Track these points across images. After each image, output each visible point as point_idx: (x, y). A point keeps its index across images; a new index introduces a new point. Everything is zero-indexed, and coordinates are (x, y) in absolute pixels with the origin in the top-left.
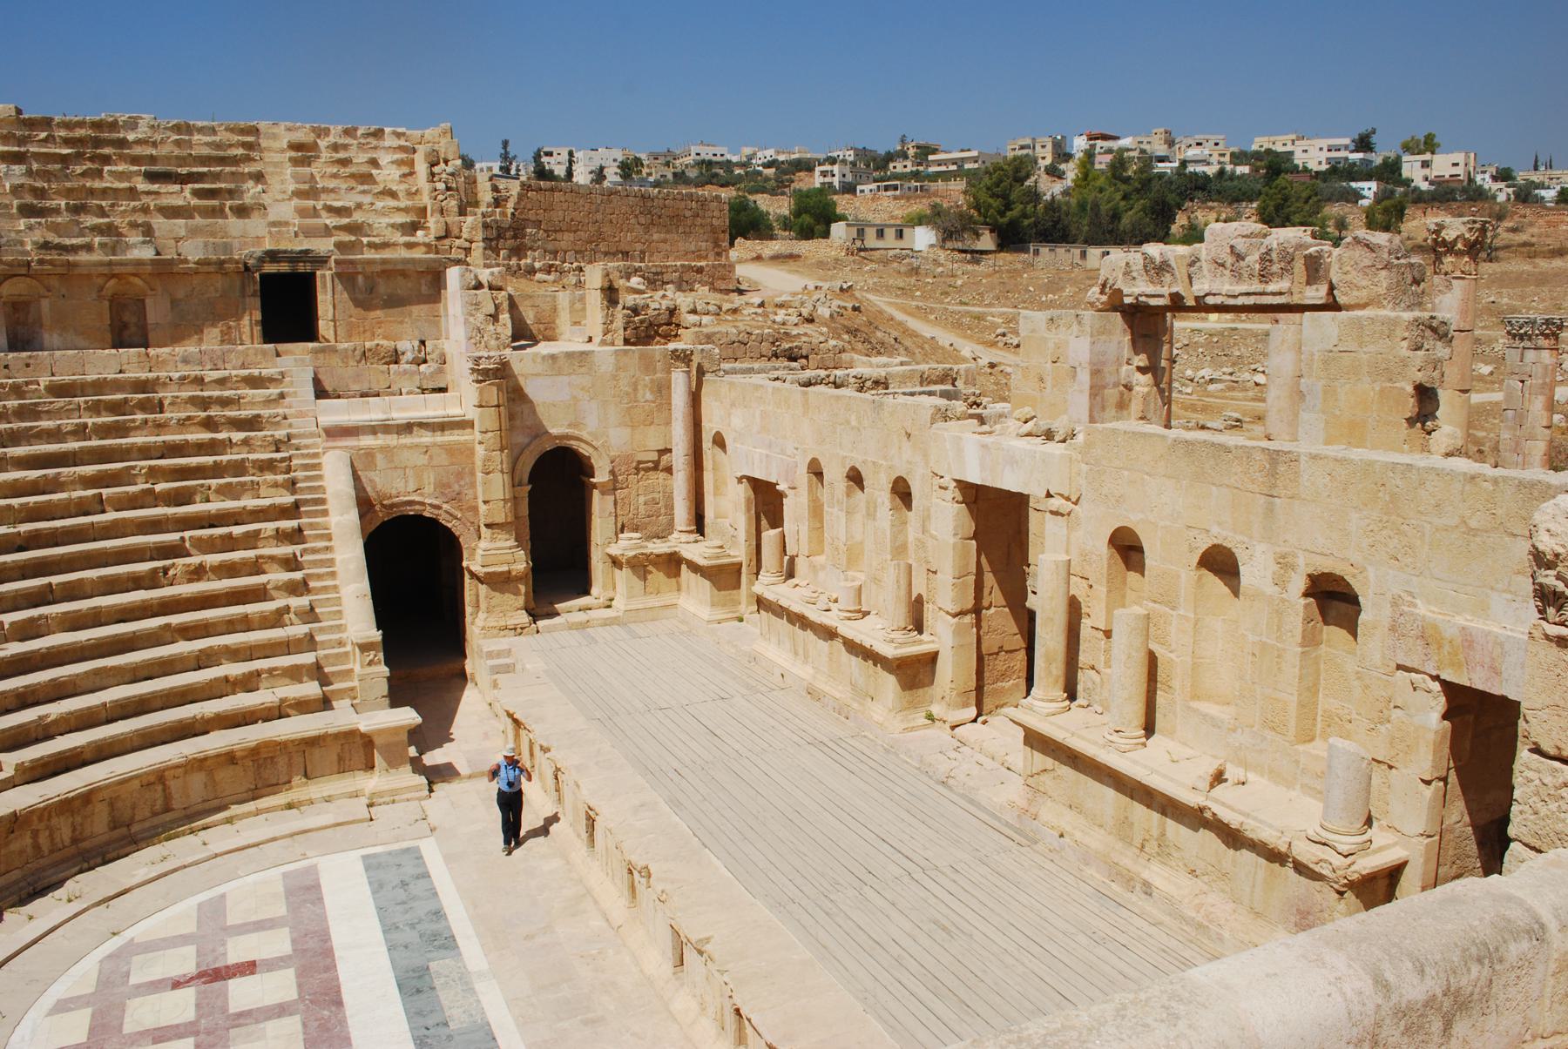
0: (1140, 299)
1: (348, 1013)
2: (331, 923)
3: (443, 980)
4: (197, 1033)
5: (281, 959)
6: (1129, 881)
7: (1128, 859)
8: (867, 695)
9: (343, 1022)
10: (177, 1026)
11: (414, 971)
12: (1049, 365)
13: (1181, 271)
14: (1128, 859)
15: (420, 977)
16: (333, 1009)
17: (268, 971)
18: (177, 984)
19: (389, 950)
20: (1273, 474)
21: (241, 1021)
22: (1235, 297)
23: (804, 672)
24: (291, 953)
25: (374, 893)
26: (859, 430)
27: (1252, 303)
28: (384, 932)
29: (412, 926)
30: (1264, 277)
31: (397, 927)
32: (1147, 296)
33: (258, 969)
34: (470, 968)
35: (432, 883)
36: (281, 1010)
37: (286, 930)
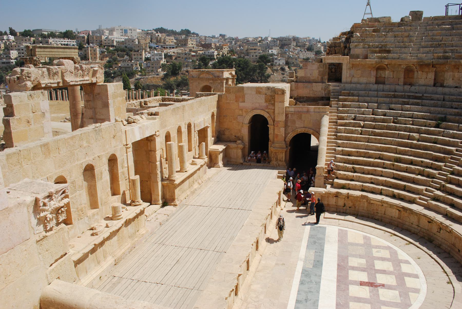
0: (48, 85)
1: (337, 262)
2: (335, 292)
3: (311, 262)
5: (352, 284)
8: (136, 232)
9: (338, 260)
10: (380, 273)
11: (317, 267)
12: (31, 115)
13: (60, 74)
15: (316, 265)
16: (340, 264)
17: (357, 281)
19: (321, 276)
22: (77, 82)
23: (110, 260)
24: (350, 285)
25: (318, 300)
26: (89, 146)
27: (82, 83)
28: (320, 282)
29: (311, 281)
30: (83, 76)
31: (316, 283)
32: (51, 83)
33: (359, 282)
34: (303, 262)
35: (297, 297)
36: (353, 268)
37: (350, 295)
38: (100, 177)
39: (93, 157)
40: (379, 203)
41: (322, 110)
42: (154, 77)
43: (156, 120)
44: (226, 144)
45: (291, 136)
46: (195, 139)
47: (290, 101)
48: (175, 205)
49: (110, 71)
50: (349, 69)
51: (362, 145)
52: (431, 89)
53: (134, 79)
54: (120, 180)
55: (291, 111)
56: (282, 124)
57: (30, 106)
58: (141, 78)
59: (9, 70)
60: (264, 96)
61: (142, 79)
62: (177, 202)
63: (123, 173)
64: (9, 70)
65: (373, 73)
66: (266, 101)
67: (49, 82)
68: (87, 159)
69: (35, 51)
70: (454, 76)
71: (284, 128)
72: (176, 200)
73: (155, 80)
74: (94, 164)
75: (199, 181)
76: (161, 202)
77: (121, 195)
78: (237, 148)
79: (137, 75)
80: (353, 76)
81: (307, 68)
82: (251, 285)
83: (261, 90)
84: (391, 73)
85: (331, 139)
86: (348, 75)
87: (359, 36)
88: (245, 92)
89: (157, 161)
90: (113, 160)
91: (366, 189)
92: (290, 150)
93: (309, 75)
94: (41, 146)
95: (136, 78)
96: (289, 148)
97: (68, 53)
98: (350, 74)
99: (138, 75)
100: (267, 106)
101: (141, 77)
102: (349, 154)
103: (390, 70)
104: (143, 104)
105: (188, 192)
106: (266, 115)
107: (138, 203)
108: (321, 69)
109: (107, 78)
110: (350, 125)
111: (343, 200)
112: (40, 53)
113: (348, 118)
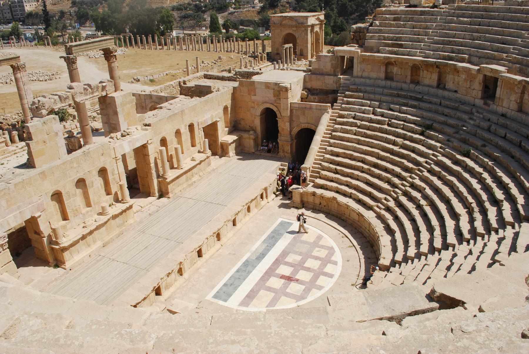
4: (303, 267)
6: (192, 184)
7: (190, 182)
8: (124, 223)
10: (304, 270)
12: (46, 136)
13: (71, 97)
14: (190, 182)
18: (297, 280)
20: (182, 114)
21: (294, 265)
23: (99, 243)
30: (92, 93)
38: (91, 185)
39: (84, 173)
40: (345, 206)
41: (323, 108)
42: (249, 11)
43: (148, 132)
44: (240, 134)
45: (295, 130)
46: (200, 135)
47: (302, 94)
48: (169, 198)
49: (200, 5)
50: (360, 63)
51: (351, 146)
52: (432, 91)
53: (227, 13)
54: (111, 184)
55: (296, 107)
56: (287, 119)
57: (45, 130)
58: (235, 12)
59: (94, 5)
60: (272, 90)
61: (236, 14)
62: (170, 195)
63: (114, 179)
64: (94, 5)
65: (383, 69)
66: (274, 96)
67: (61, 106)
68: (78, 175)
69: (72, 50)
70: (454, 79)
71: (289, 123)
72: (170, 194)
73: (250, 14)
74: (84, 178)
75: (200, 174)
76: (157, 194)
77: (113, 195)
78: (249, 138)
79: (230, 8)
80: (364, 71)
81: (320, 60)
82: (200, 268)
83: (269, 85)
84: (399, 70)
85: (326, 137)
86: (359, 69)
87: (378, 24)
88: (256, 86)
89: (151, 163)
90: (103, 172)
91: (340, 191)
92: (296, 142)
93: (322, 67)
94: (39, 174)
95: (230, 12)
96: (295, 141)
97: (104, 45)
98: (361, 68)
99: (232, 8)
100: (275, 100)
101: (234, 10)
102: (337, 155)
103: (398, 66)
104: (182, 84)
105: (185, 185)
106: (275, 109)
107: (125, 202)
108: (333, 62)
109: (197, 12)
110: (348, 124)
111: (319, 199)
112: (76, 51)
113: (348, 117)
